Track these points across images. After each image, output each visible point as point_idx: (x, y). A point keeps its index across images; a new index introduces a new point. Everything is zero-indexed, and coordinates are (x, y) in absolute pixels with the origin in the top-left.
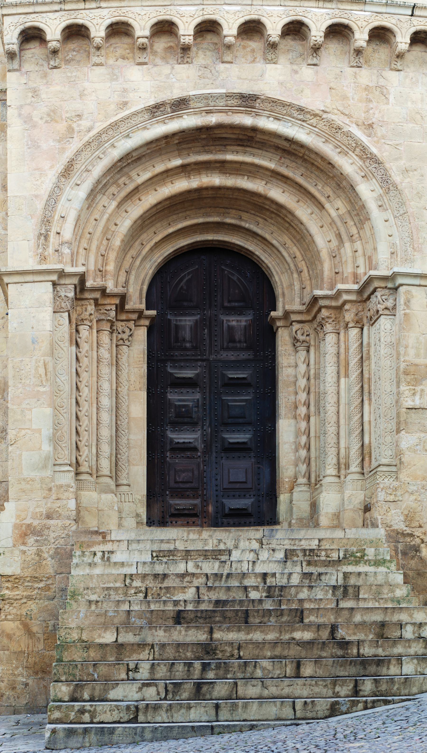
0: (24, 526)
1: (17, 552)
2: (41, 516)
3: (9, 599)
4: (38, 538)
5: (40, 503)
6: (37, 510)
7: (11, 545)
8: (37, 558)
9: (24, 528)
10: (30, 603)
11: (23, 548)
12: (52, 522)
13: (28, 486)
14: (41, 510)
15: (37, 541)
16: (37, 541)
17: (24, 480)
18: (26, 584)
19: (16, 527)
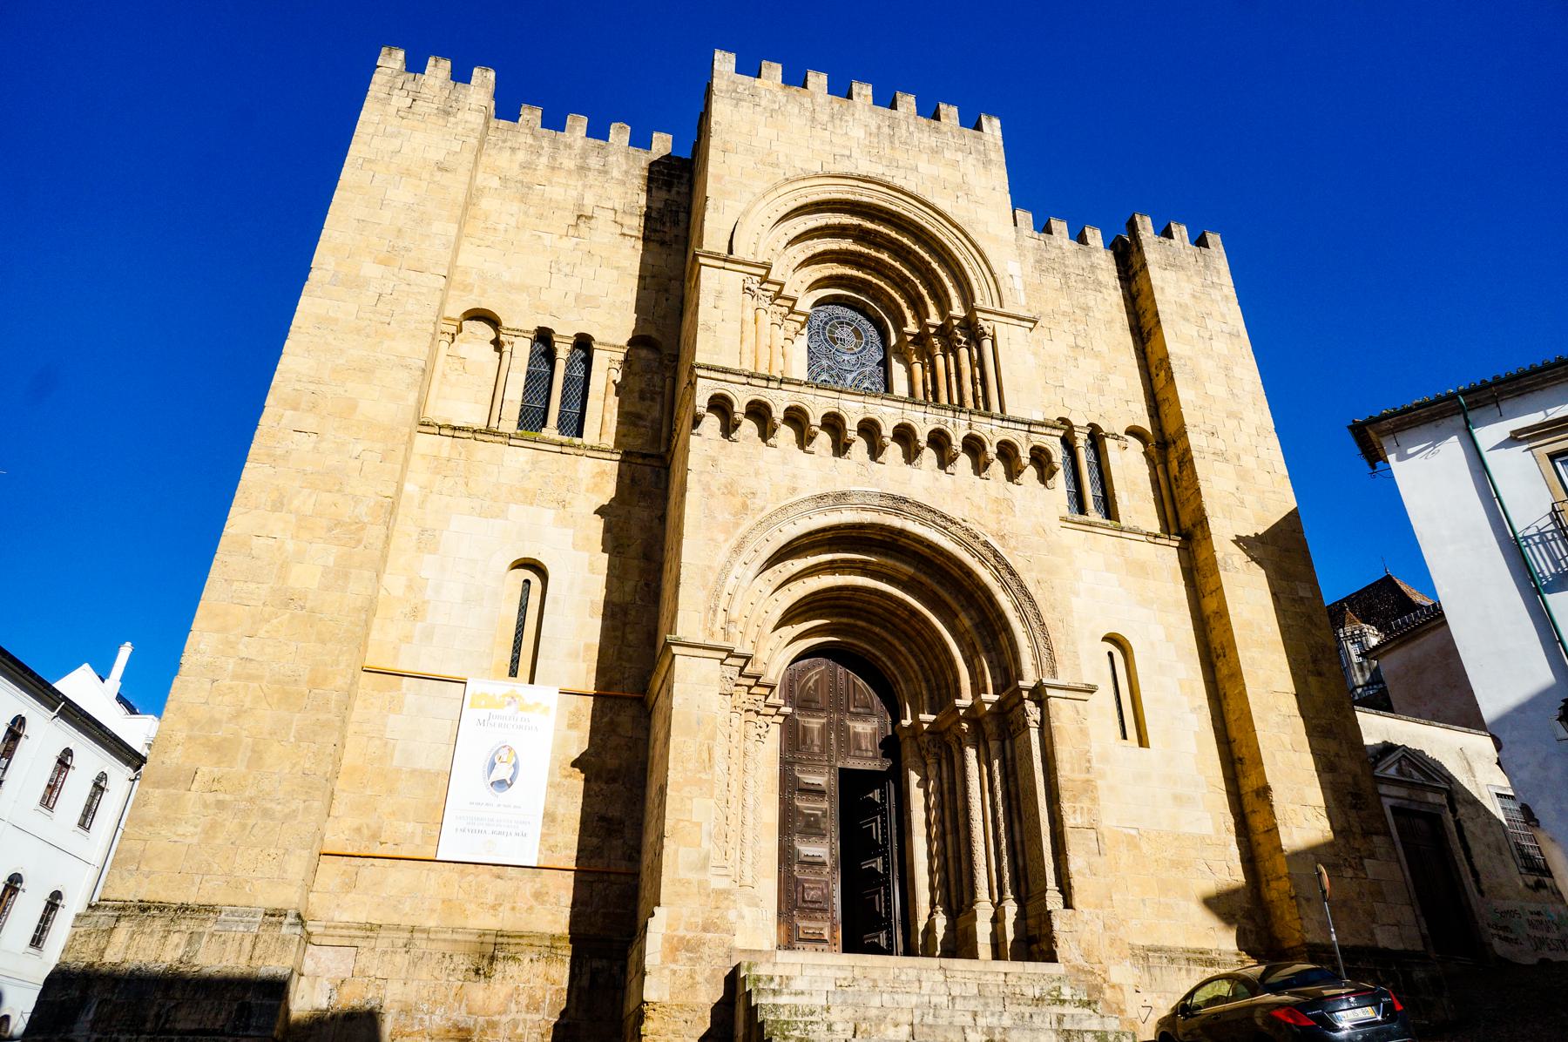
0: (676, 939)
1: (667, 972)
4: (691, 955)
6: (693, 920)
8: (690, 981)
11: (673, 966)
12: (709, 936)
14: (697, 920)
15: (690, 959)
19: (668, 939)
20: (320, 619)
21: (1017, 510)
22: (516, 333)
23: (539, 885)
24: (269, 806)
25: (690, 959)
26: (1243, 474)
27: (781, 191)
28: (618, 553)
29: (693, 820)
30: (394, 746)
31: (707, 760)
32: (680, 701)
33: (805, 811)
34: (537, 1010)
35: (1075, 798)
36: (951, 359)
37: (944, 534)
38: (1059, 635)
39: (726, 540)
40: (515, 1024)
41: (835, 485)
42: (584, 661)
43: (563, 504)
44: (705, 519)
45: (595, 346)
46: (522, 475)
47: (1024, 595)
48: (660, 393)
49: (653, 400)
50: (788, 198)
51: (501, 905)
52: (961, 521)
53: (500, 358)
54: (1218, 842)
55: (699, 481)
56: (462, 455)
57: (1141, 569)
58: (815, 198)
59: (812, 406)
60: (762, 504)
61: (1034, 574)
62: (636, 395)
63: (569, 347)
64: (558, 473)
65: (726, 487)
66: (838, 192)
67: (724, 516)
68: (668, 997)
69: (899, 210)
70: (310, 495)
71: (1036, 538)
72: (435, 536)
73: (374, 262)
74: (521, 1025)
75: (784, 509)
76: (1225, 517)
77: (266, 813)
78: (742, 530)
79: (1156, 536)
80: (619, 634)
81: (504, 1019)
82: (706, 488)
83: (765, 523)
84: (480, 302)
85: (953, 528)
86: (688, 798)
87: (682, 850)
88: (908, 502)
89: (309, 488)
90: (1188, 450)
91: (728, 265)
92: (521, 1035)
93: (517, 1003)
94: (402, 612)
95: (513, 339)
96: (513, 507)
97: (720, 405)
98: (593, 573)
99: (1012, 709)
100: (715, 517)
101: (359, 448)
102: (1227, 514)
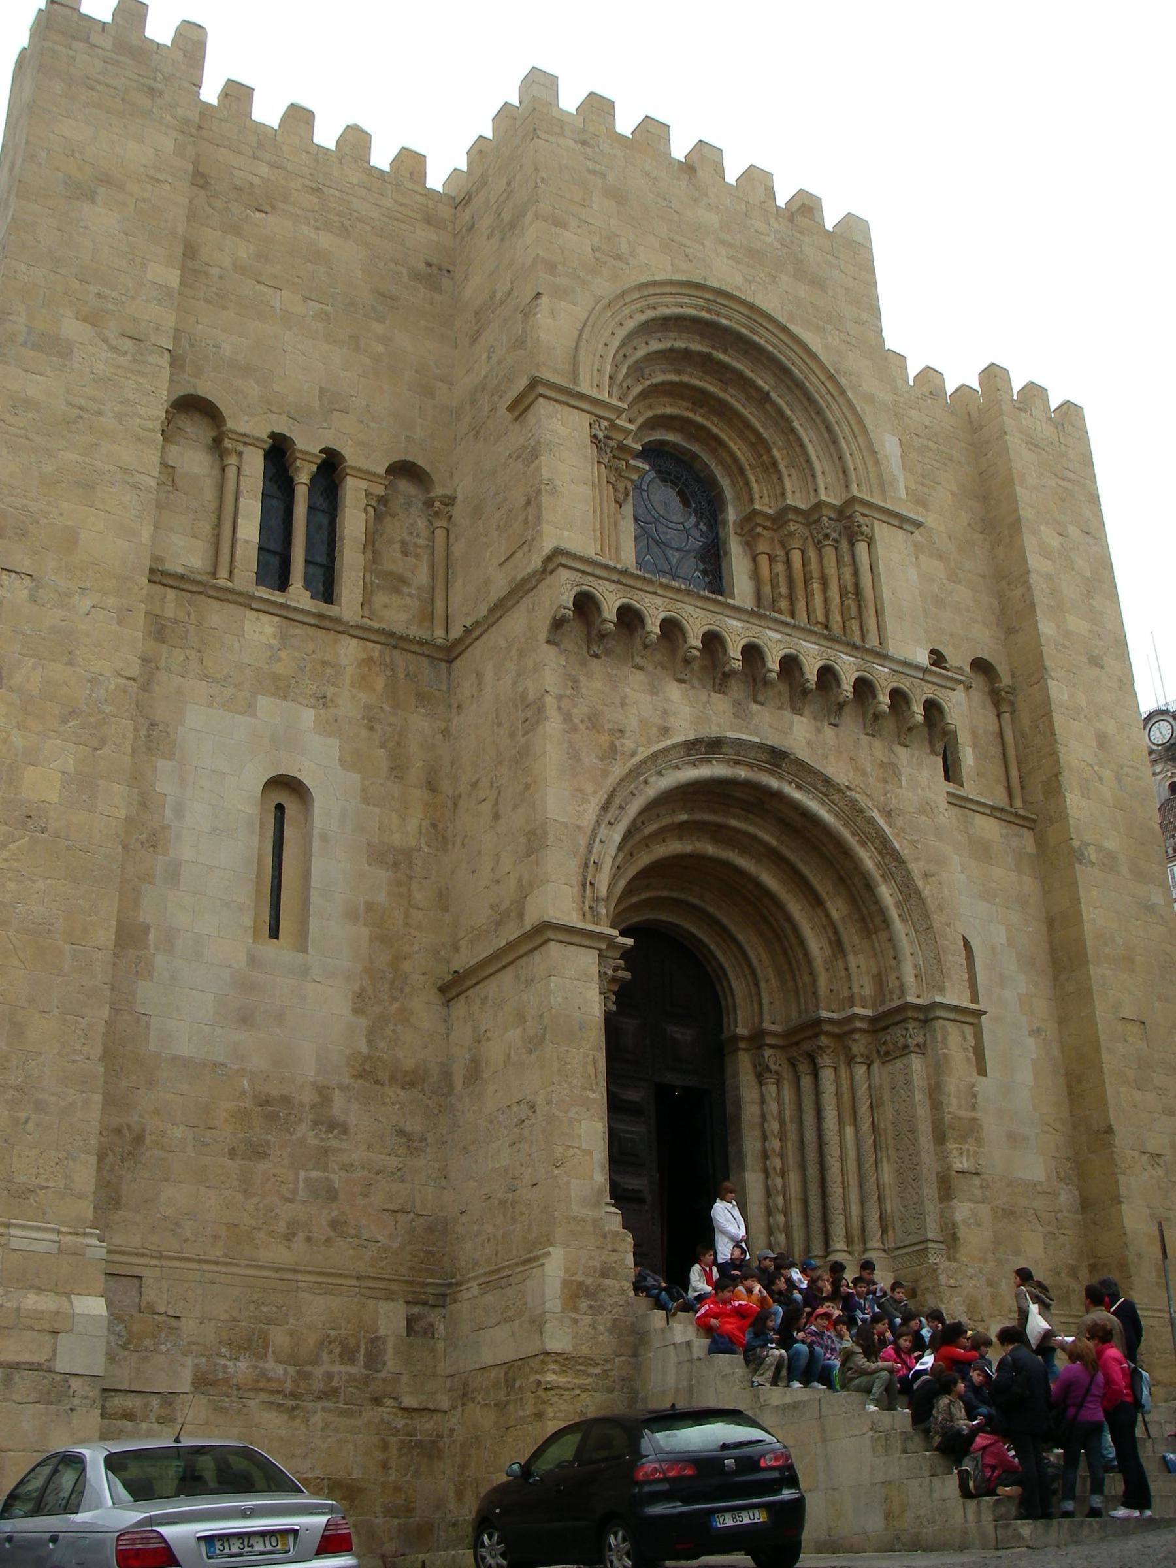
1: (567, 1321)
2: (595, 1272)
3: (560, 1388)
5: (593, 1253)
6: (591, 1263)
7: (559, 1310)
8: (592, 1332)
9: (574, 1287)
10: (584, 1395)
11: (573, 1315)
12: (608, 1282)
13: (579, 1228)
16: (590, 1307)
17: (574, 1218)
18: (578, 1368)
19: (565, 1283)
20: (68, 848)
21: (903, 779)
22: (246, 440)
23: (335, 1213)
24: (41, 1096)
25: (590, 1307)
26: (1102, 741)
27: (628, 299)
28: (396, 777)
29: (584, 1147)
30: (148, 1025)
31: (593, 1077)
32: (559, 1000)
33: (622, 1135)
34: (352, 1360)
35: (962, 1139)
36: (812, 554)
37: (822, 802)
38: (947, 943)
39: (595, 792)
40: (330, 1376)
41: (710, 728)
42: (365, 925)
43: (323, 701)
44: (570, 761)
45: (348, 471)
46: (269, 654)
47: (909, 893)
48: (427, 546)
49: (417, 556)
50: (633, 307)
51: (294, 1235)
52: (842, 787)
53: (223, 470)
54: (1049, 1191)
55: (559, 708)
56: (192, 617)
57: (982, 851)
58: (667, 311)
59: (691, 621)
60: (632, 746)
61: (921, 864)
62: (397, 546)
63: (314, 469)
64: (314, 656)
65: (590, 719)
66: (690, 306)
67: (590, 760)
68: (571, 1349)
69: (762, 342)
70: (34, 668)
71: (924, 818)
72: (168, 733)
73: (77, 319)
74: (336, 1378)
75: (655, 756)
76: (1083, 796)
77: (40, 1107)
78: (612, 780)
79: (1002, 810)
80: (404, 890)
81: (319, 1371)
82: (567, 718)
83: (634, 774)
84: (194, 386)
85: (836, 797)
86: (575, 1119)
87: (572, 1180)
88: (788, 757)
89: (31, 656)
90: (1047, 701)
91: (573, 402)
92: (337, 1388)
93: (330, 1353)
94: (137, 839)
95: (240, 448)
96: (263, 701)
97: (585, 604)
98: (368, 804)
99: (886, 1028)
100: (580, 760)
101: (87, 603)
102: (1085, 793)
